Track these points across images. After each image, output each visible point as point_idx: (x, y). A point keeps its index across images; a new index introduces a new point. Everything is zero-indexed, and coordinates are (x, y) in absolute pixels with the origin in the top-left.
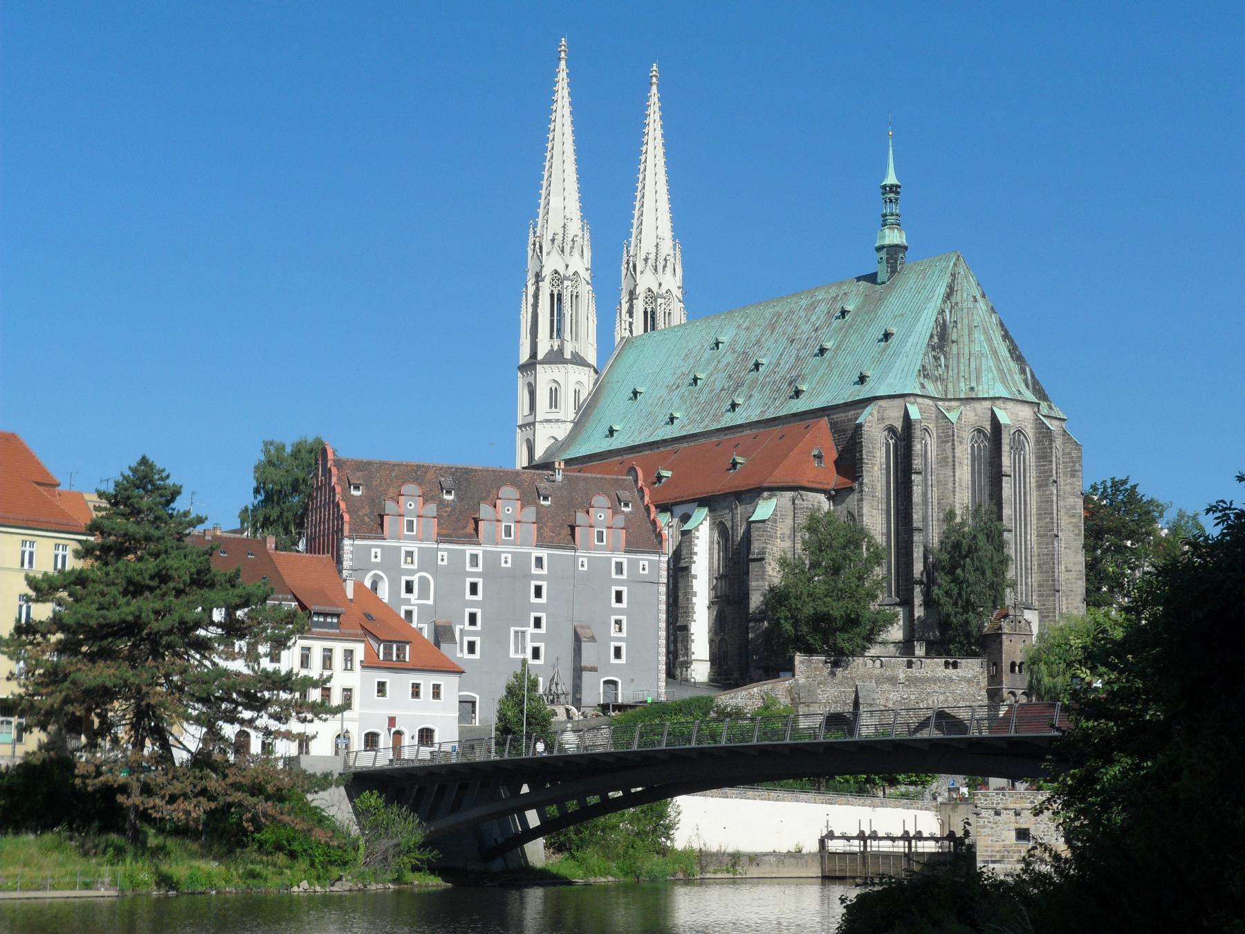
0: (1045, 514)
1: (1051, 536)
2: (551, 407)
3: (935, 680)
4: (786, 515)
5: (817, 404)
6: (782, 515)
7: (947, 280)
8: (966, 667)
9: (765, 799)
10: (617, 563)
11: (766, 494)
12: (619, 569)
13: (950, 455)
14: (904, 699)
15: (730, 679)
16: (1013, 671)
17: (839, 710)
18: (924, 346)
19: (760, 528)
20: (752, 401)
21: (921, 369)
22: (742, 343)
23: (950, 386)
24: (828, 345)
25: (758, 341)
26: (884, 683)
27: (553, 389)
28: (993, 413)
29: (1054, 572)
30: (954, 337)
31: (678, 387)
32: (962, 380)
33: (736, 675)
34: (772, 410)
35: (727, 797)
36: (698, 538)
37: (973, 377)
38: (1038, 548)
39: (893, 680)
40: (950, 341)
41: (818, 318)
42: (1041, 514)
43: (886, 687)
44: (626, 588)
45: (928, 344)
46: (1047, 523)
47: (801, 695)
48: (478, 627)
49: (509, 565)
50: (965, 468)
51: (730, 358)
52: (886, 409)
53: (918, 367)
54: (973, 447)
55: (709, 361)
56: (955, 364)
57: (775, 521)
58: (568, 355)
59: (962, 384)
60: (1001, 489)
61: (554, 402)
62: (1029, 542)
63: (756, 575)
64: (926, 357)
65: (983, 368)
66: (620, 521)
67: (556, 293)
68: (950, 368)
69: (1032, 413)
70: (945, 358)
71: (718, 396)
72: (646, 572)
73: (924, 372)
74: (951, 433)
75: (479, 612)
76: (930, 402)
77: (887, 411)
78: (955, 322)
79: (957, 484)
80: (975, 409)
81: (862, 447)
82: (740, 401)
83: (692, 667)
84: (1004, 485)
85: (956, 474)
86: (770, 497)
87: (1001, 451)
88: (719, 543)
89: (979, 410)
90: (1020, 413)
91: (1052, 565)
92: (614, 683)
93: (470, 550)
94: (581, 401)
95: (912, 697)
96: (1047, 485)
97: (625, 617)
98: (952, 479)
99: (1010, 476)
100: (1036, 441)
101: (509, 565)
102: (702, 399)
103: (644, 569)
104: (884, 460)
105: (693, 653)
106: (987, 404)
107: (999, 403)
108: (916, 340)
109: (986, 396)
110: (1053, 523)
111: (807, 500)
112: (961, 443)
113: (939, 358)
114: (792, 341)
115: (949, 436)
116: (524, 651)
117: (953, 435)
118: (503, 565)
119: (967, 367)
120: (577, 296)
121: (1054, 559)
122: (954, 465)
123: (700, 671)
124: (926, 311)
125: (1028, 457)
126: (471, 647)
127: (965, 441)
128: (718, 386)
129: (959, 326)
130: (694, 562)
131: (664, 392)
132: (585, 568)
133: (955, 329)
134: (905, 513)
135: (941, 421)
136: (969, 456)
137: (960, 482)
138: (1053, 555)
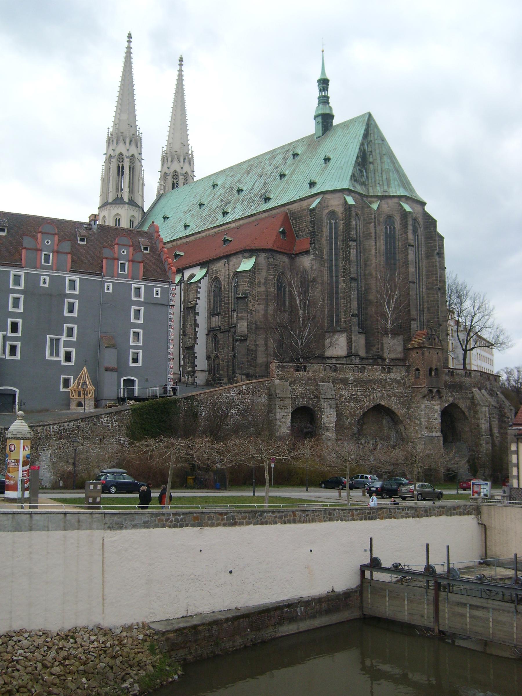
0: (432, 274)
3: (374, 381)
4: (262, 269)
6: (259, 269)
7: (364, 127)
8: (396, 372)
9: (289, 522)
10: (136, 288)
11: (246, 255)
12: (138, 295)
13: (372, 230)
14: (353, 395)
15: (221, 383)
16: (430, 374)
18: (353, 162)
19: (243, 276)
20: (236, 210)
22: (229, 183)
23: (371, 189)
24: (286, 173)
25: (239, 181)
26: (338, 383)
27: (118, 219)
28: (400, 204)
29: (438, 312)
30: (371, 160)
31: (190, 211)
32: (378, 185)
33: (225, 380)
34: (250, 211)
35: (235, 524)
36: (200, 288)
37: (385, 183)
38: (427, 297)
39: (345, 382)
41: (278, 162)
43: (340, 386)
46: (433, 280)
48: (19, 334)
49: (47, 285)
50: (382, 241)
51: (222, 191)
52: (330, 200)
53: (350, 174)
54: (386, 228)
55: (209, 196)
56: (373, 176)
57: (254, 273)
58: (126, 199)
59: (378, 188)
60: (407, 255)
62: (421, 293)
63: (241, 309)
64: (355, 169)
65: (391, 178)
66: (139, 257)
67: (121, 166)
68: (370, 178)
69: (421, 209)
70: (366, 172)
71: (214, 211)
72: (159, 296)
73: (354, 178)
74: (373, 217)
75: (20, 321)
76: (359, 197)
78: (371, 152)
79: (378, 251)
80: (388, 204)
81: (314, 224)
82: (229, 210)
83: (195, 375)
85: (377, 244)
86: (250, 257)
87: (407, 229)
88: (214, 292)
90: (416, 208)
91: (437, 308)
92: (133, 381)
93: (13, 272)
95: (359, 394)
96: (433, 256)
98: (374, 247)
99: (413, 246)
101: (47, 285)
102: (204, 214)
103: (157, 294)
104: (328, 234)
105: (196, 366)
106: (396, 200)
107: (403, 199)
108: (347, 160)
109: (395, 194)
110: (437, 280)
111: (276, 260)
112: (379, 224)
114: (261, 176)
115: (372, 219)
116: (57, 355)
118: (42, 285)
119: (381, 178)
120: (133, 169)
121: (437, 304)
122: (376, 238)
123: (201, 378)
125: (420, 237)
126: (13, 349)
127: (381, 224)
128: (214, 206)
129: (374, 154)
130: (198, 304)
131: (182, 215)
132: (110, 291)
133: (371, 156)
134: (344, 269)
135: (366, 209)
136: (384, 234)
137: (379, 249)
138: (438, 301)
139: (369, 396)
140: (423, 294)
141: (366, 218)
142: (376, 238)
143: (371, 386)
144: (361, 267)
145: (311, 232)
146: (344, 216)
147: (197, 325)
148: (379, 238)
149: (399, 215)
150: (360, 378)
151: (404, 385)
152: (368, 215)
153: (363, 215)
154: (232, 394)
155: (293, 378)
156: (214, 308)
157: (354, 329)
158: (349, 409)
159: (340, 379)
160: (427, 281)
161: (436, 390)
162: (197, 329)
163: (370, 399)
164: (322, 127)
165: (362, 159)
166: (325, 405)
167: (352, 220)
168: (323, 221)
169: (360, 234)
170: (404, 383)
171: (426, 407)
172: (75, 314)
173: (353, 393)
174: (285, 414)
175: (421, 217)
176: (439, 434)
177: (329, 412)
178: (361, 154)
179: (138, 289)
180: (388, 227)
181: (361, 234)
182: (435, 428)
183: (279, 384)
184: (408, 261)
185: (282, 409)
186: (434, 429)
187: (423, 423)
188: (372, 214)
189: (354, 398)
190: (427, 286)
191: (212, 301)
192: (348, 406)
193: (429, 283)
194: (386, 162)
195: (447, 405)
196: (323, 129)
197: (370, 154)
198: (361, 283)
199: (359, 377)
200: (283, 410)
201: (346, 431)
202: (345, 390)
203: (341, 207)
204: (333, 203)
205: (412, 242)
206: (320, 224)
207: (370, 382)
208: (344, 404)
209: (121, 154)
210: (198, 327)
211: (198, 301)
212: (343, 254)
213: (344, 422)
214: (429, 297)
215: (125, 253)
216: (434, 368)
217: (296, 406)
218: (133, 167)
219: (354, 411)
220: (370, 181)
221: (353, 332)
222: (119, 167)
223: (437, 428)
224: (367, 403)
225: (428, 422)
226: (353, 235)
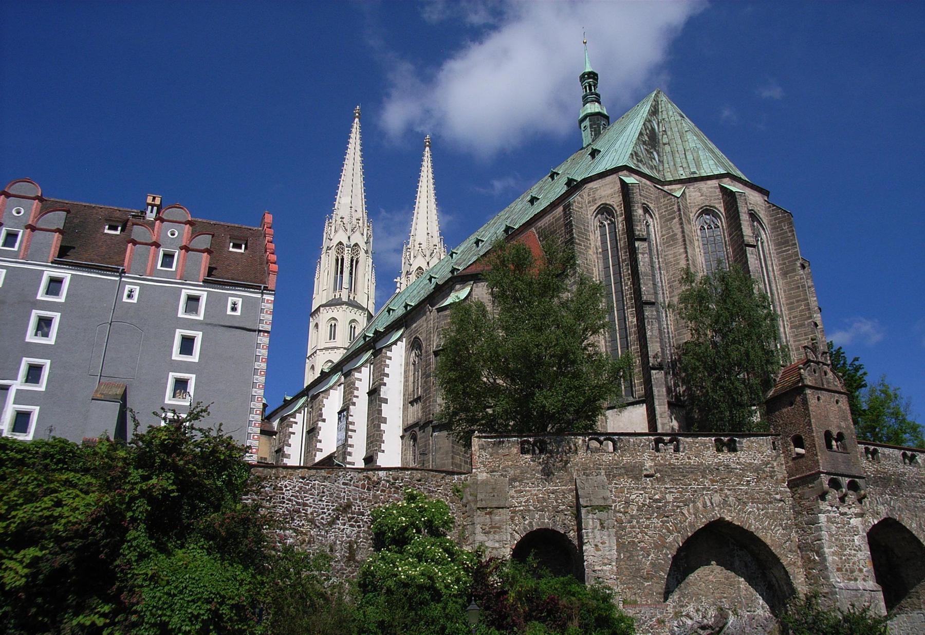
0: (798, 301)
1: (809, 324)
2: (330, 339)
3: (704, 471)
5: (524, 221)
13: (677, 230)
16: (829, 446)
17: (547, 522)
21: (633, 153)
27: (333, 325)
30: (665, 140)
36: (390, 358)
38: (795, 341)
39: (635, 472)
40: (661, 145)
42: (793, 303)
44: (200, 334)
45: (638, 138)
46: (801, 311)
47: (480, 497)
52: (597, 189)
56: (670, 158)
61: (332, 336)
69: (763, 201)
70: (659, 155)
72: (238, 313)
76: (648, 183)
77: (598, 193)
78: (665, 131)
79: (690, 262)
80: (700, 190)
81: (572, 225)
84: (748, 255)
85: (688, 250)
89: (705, 189)
90: (751, 197)
94: (356, 335)
95: (670, 498)
96: (794, 270)
97: (193, 376)
98: (685, 255)
99: (754, 246)
100: (772, 229)
103: (234, 309)
104: (599, 244)
106: (714, 183)
108: (625, 140)
113: (652, 153)
115: (674, 212)
117: (679, 210)
119: (684, 160)
122: (684, 240)
124: (632, 124)
125: (765, 244)
129: (669, 133)
130: (385, 384)
135: (662, 200)
136: (700, 239)
139: (694, 502)
140: (786, 338)
141: (664, 213)
142: (684, 240)
143: (694, 480)
144: (663, 293)
145: (568, 242)
146: (623, 208)
147: (384, 421)
148: (691, 242)
149: (722, 204)
150: (670, 464)
151: (772, 477)
152: (667, 207)
153: (658, 211)
154: (344, 484)
155: (516, 467)
156: (414, 391)
157: (659, 391)
158: (650, 533)
159: (624, 467)
160: (790, 314)
161: (847, 480)
162: (383, 426)
163: (696, 509)
164: (591, 131)
165: (649, 138)
166: (590, 521)
167: (636, 208)
168: (588, 223)
169: (656, 239)
170: (771, 472)
171: (829, 520)
172: (51, 340)
173: (657, 497)
174: (497, 545)
175: (763, 212)
176: (871, 584)
177: (598, 536)
178: (648, 131)
179: (193, 300)
180: (706, 227)
181: (658, 240)
182: (861, 570)
183: (485, 483)
184: (749, 272)
185: (489, 533)
186: (856, 573)
187: (830, 559)
188: (674, 204)
189: (659, 508)
190: (791, 323)
191: (411, 379)
192: (647, 527)
193: (794, 317)
194: (690, 141)
195: (876, 522)
196: (593, 133)
197: (663, 134)
198: (667, 320)
199: (666, 461)
200: (491, 536)
201: (646, 584)
202: (638, 489)
203: (617, 195)
204: (603, 194)
205: (752, 241)
206: (583, 227)
207: (692, 472)
208: (638, 522)
209: (341, 243)
210: (386, 423)
211: (386, 380)
212: (628, 269)
213: (640, 562)
214: (800, 340)
215: (176, 234)
216: (835, 433)
217: (525, 528)
218: (357, 259)
219: (663, 537)
220: (666, 165)
221: (656, 397)
222: (337, 260)
223: (865, 570)
224: (691, 518)
225: (840, 555)
226: (641, 231)
